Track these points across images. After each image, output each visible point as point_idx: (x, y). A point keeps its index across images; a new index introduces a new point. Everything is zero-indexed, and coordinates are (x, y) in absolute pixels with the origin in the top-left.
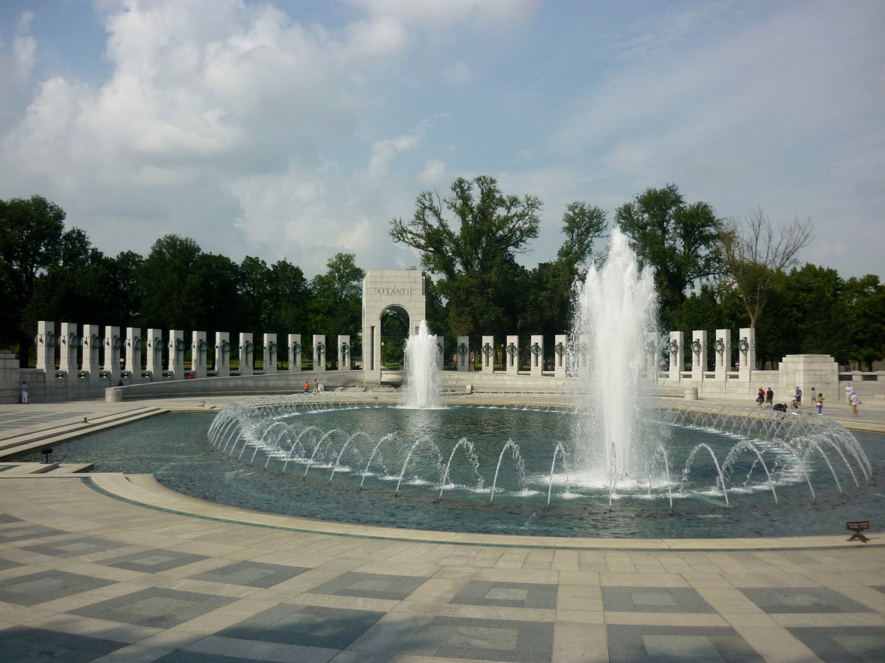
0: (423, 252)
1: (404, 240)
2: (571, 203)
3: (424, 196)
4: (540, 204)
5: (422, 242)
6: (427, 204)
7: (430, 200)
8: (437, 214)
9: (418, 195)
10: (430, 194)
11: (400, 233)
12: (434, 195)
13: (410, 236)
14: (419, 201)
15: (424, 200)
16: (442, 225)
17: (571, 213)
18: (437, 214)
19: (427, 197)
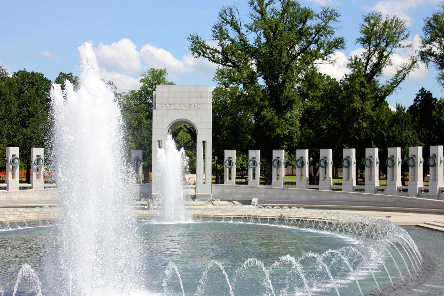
0: (221, 67)
1: (203, 56)
2: (366, 14)
3: (225, 12)
4: (337, 15)
5: (220, 56)
6: (229, 19)
7: (232, 14)
8: (238, 30)
9: (219, 10)
10: (231, 9)
11: (198, 48)
12: (234, 10)
13: (208, 51)
14: (221, 16)
15: (224, 16)
16: (241, 40)
17: (366, 24)
18: (238, 30)
19: (228, 12)
